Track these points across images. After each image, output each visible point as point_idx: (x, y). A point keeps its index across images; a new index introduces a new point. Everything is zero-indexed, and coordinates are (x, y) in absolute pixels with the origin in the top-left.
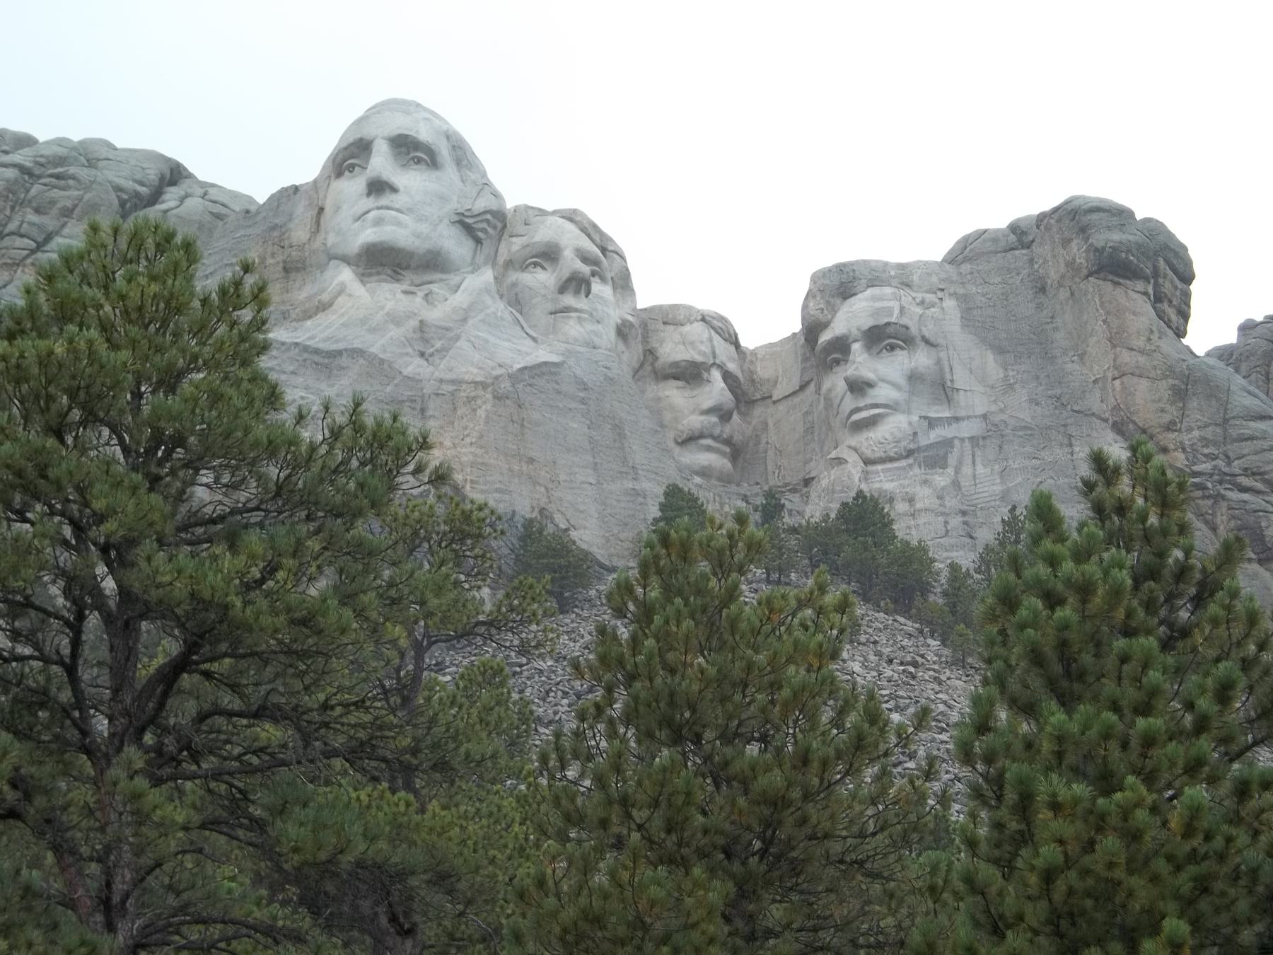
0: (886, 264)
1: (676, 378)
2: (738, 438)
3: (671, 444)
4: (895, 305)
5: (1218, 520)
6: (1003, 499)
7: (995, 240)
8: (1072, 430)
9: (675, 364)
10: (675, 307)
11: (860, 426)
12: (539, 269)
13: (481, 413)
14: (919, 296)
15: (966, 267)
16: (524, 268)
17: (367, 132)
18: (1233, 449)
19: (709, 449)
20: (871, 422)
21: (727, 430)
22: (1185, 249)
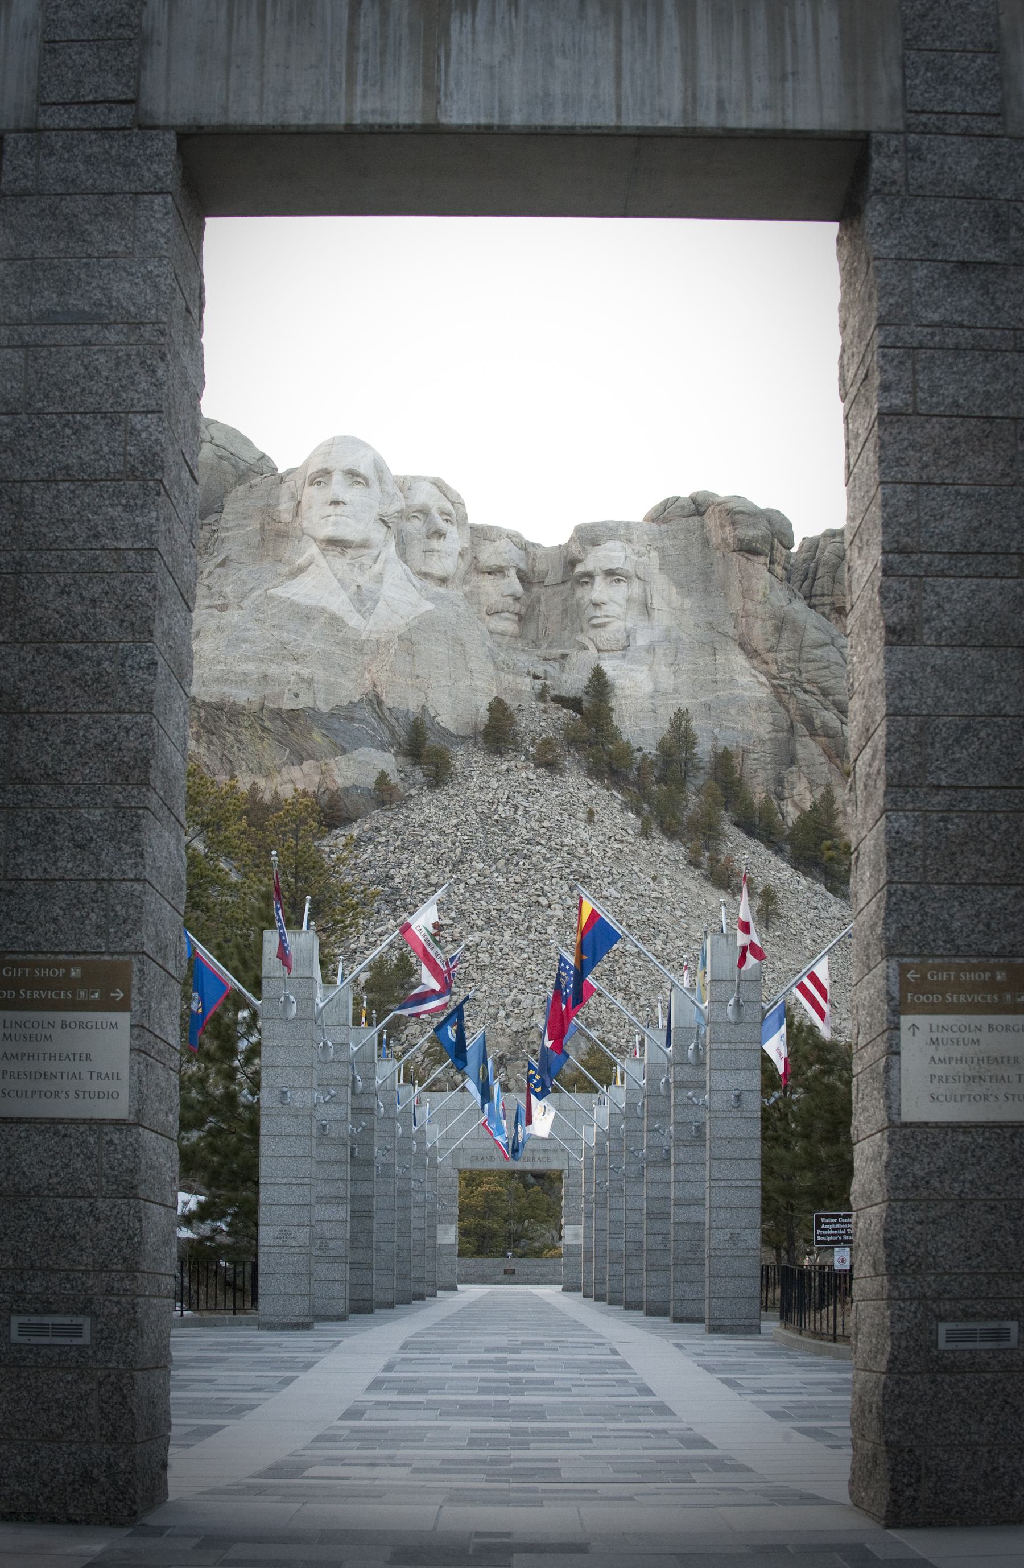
0: (619, 524)
1: (489, 573)
2: (523, 611)
3: (484, 615)
4: (622, 555)
5: (791, 707)
6: (676, 690)
7: (683, 508)
8: (717, 645)
9: (490, 567)
10: (491, 528)
11: (595, 626)
12: (416, 521)
13: (392, 651)
14: (637, 548)
15: (664, 526)
16: (408, 519)
17: (328, 465)
18: (803, 666)
19: (507, 619)
20: (602, 625)
21: (517, 607)
22: (790, 525)
